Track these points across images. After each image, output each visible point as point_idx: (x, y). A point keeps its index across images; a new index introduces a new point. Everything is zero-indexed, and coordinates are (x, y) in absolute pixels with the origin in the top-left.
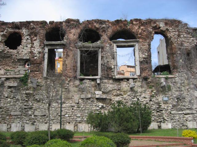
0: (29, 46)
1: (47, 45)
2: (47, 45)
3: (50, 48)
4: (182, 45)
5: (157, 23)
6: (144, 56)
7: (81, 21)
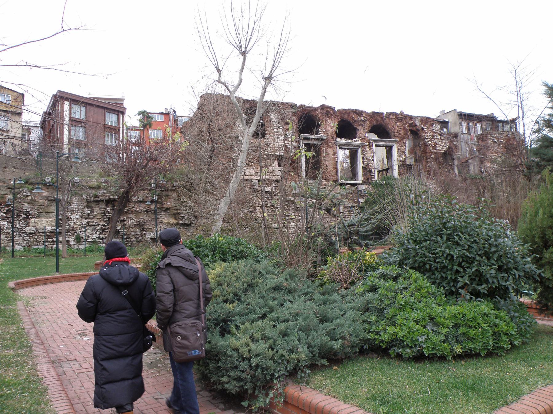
0: (282, 138)
1: (305, 139)
2: (305, 139)
3: (306, 142)
4: (435, 148)
5: (414, 120)
6: (401, 159)
7: (336, 109)
